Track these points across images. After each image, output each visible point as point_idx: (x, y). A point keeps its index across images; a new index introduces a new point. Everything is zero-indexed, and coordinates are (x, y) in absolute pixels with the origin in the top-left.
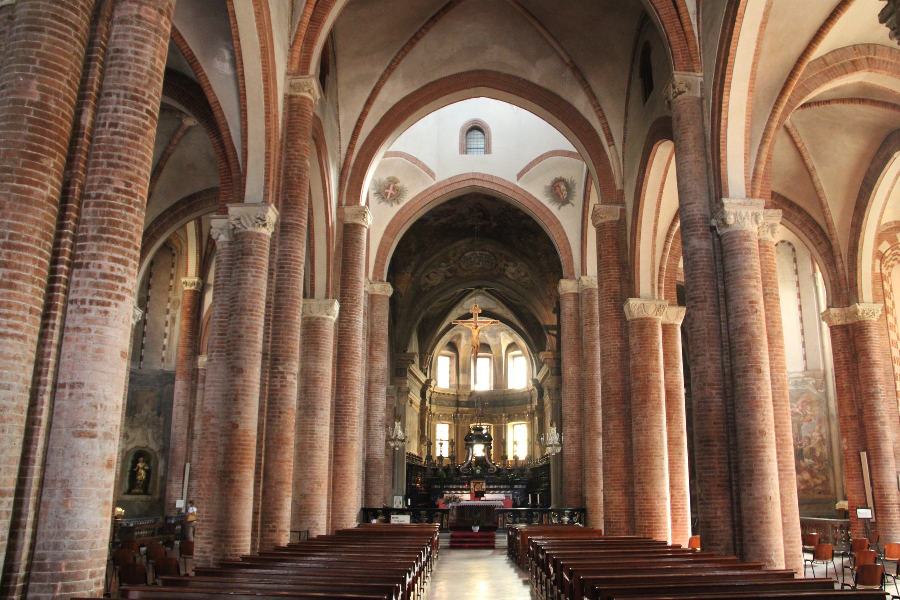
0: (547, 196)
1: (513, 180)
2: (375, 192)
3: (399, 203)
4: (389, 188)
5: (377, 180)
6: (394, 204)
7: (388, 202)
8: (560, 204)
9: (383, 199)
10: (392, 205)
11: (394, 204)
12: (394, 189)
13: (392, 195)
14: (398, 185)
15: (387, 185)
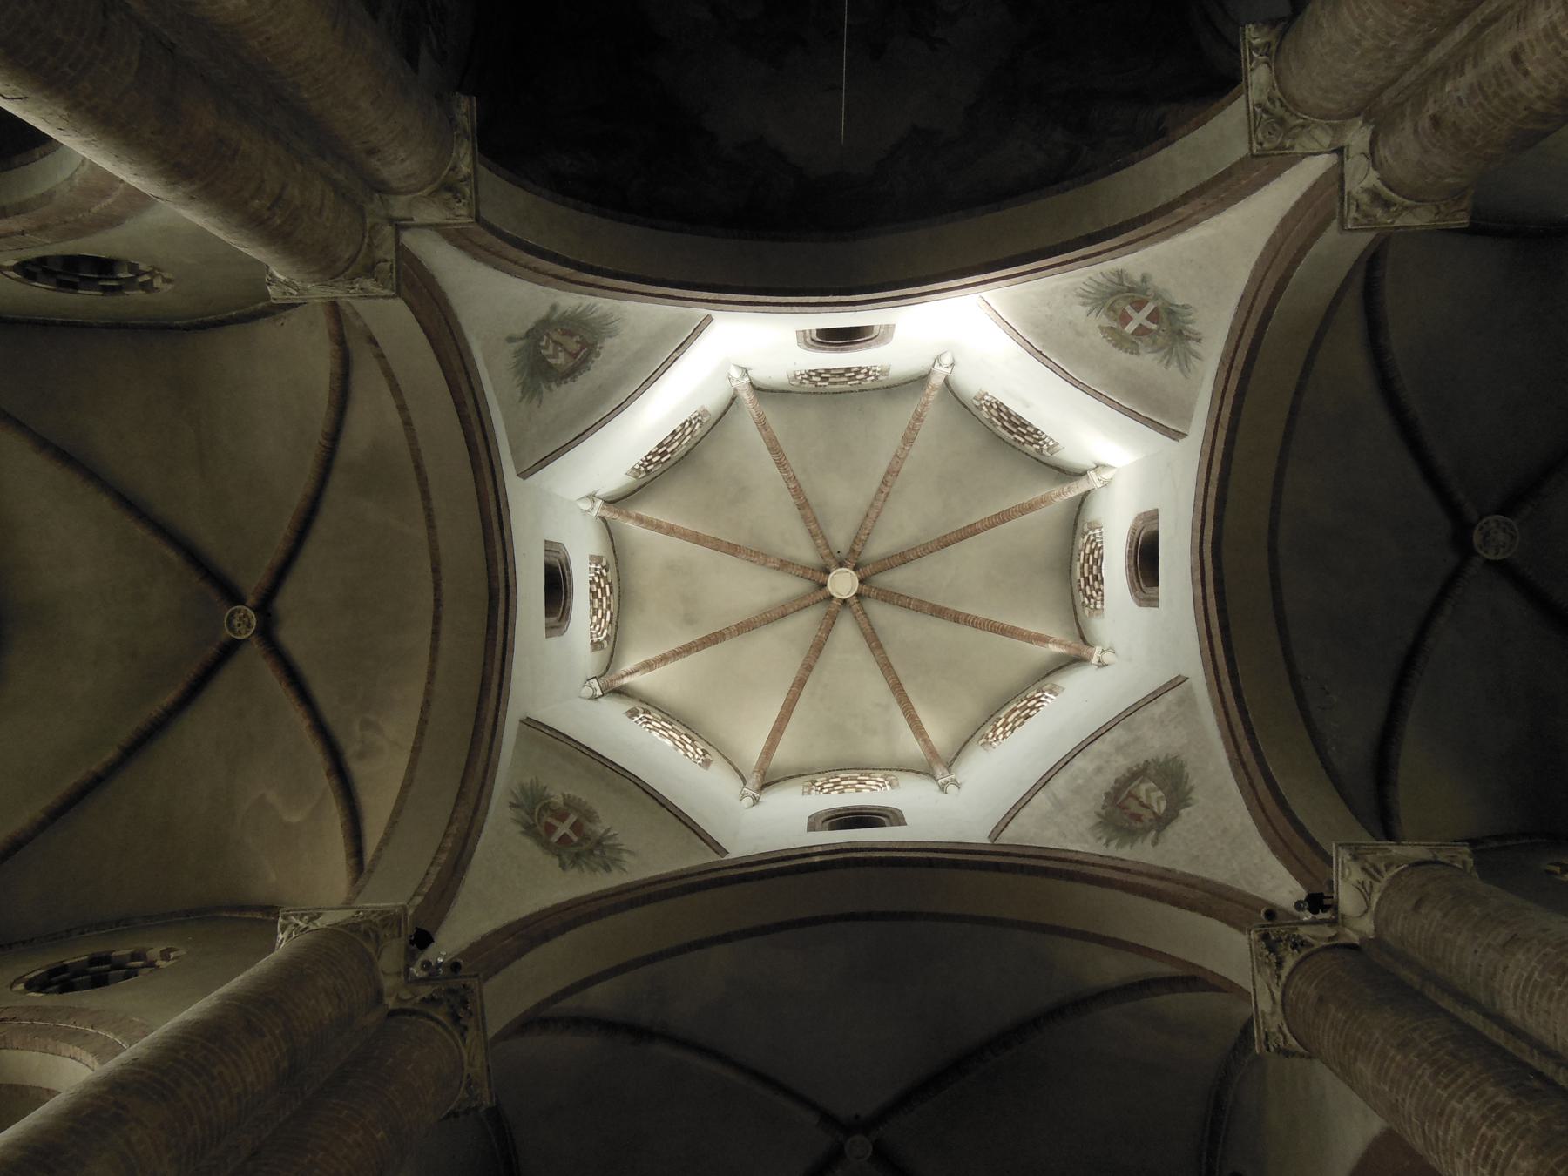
0: (605, 316)
1: (714, 314)
2: (1193, 345)
3: (1120, 274)
4: (1141, 331)
5: (1174, 368)
6: (1138, 279)
7: (1157, 297)
8: (555, 317)
9: (1171, 313)
10: (1144, 279)
11: (1138, 279)
12: (1125, 319)
13: (1139, 305)
14: (1104, 321)
15: (1146, 338)
